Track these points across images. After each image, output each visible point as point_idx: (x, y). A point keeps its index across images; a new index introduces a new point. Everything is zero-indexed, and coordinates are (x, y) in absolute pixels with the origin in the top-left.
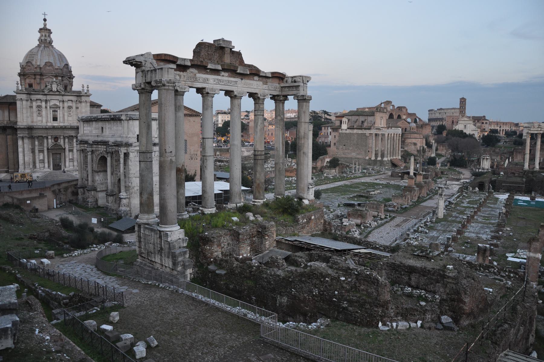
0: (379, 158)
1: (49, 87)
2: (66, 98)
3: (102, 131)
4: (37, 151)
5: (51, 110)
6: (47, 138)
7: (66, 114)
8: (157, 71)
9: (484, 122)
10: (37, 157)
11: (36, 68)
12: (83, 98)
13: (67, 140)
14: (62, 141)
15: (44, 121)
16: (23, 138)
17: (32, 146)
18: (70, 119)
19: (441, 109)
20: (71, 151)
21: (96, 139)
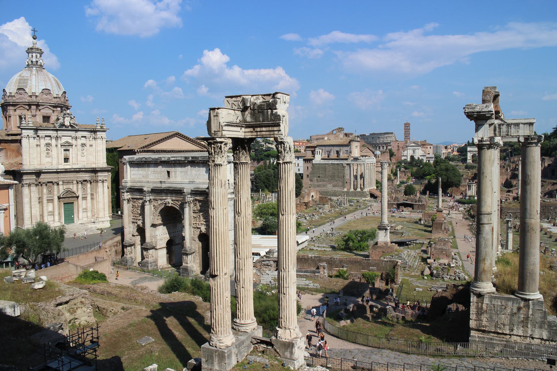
0: (359, 190)
1: (61, 121)
2: (80, 134)
3: (169, 176)
4: (45, 201)
5: (63, 149)
6: (58, 184)
7: (80, 153)
8: (521, 125)
9: (429, 147)
10: (45, 208)
11: (31, 96)
12: (98, 133)
13: (80, 185)
14: (75, 186)
15: (55, 162)
16: (29, 185)
17: (39, 195)
18: (84, 159)
19: (374, 134)
20: (85, 198)
21: (159, 185)
